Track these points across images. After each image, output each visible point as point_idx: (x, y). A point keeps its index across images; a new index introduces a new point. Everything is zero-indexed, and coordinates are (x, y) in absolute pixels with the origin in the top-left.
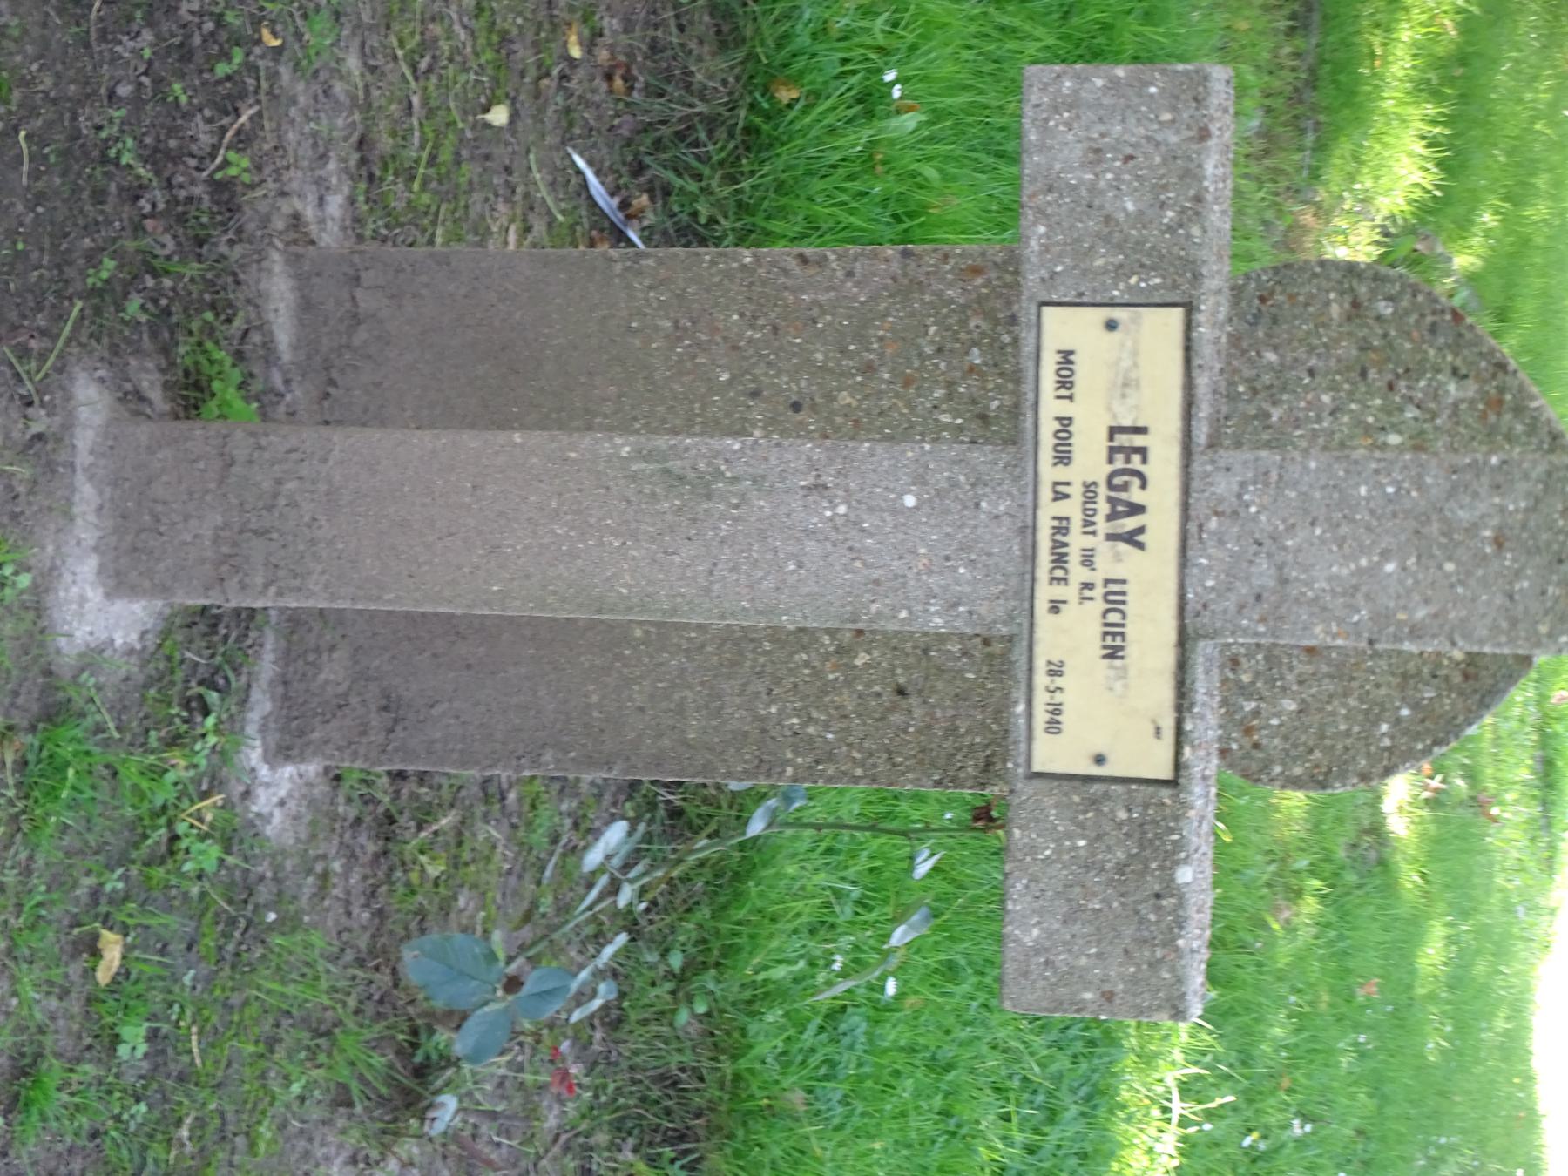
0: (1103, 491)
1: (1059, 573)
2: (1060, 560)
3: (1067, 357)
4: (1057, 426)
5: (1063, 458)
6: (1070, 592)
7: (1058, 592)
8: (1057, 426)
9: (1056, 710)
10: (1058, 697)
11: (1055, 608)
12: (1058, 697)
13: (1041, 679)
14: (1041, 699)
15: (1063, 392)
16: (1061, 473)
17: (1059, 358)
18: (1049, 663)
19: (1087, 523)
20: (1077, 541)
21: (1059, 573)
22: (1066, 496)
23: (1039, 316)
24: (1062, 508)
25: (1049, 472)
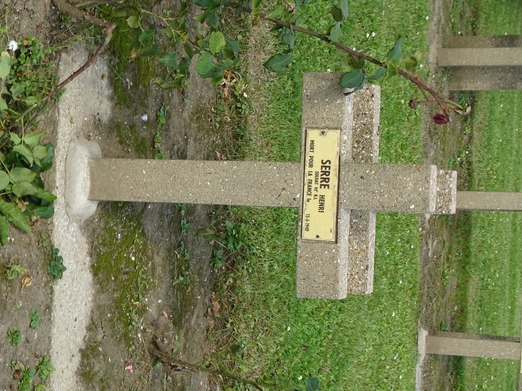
0: (320, 173)
1: (309, 193)
2: (310, 190)
3: (312, 142)
4: (310, 158)
5: (311, 166)
6: (312, 197)
7: (309, 197)
8: (310, 158)
9: (308, 225)
10: (308, 222)
11: (308, 201)
12: (308, 222)
15: (311, 150)
19: (316, 181)
20: (314, 185)
21: (309, 193)
24: (310, 178)
25: (308, 169)
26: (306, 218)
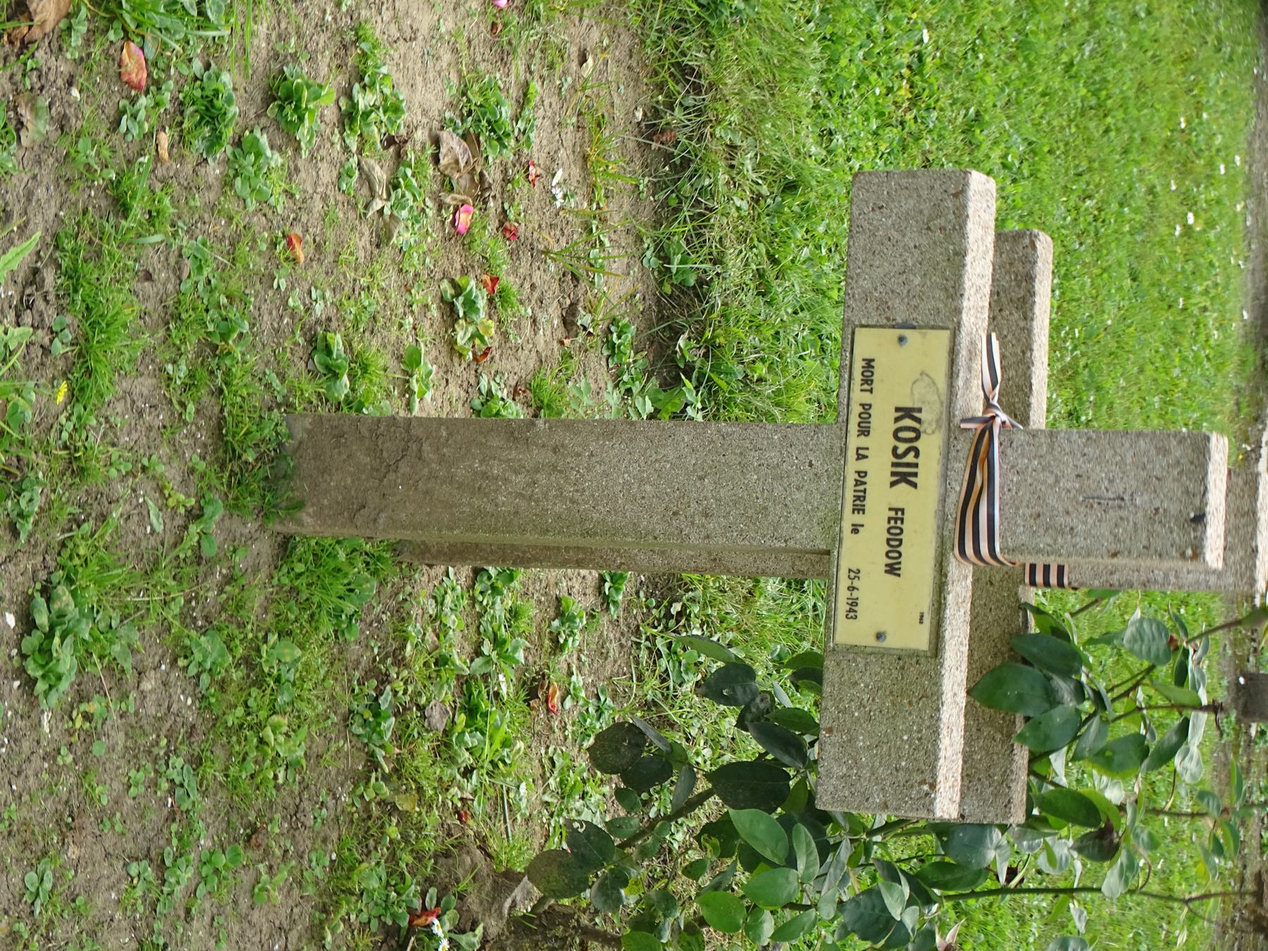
2: (860, 498)
3: (869, 363)
4: (861, 409)
5: (864, 431)
10: (855, 594)
12: (855, 594)
13: (844, 582)
14: (843, 594)
15: (866, 387)
16: (863, 441)
17: (864, 364)
18: (850, 570)
22: (866, 457)
23: (853, 333)
24: (863, 465)
25: (854, 441)
26: (848, 583)
